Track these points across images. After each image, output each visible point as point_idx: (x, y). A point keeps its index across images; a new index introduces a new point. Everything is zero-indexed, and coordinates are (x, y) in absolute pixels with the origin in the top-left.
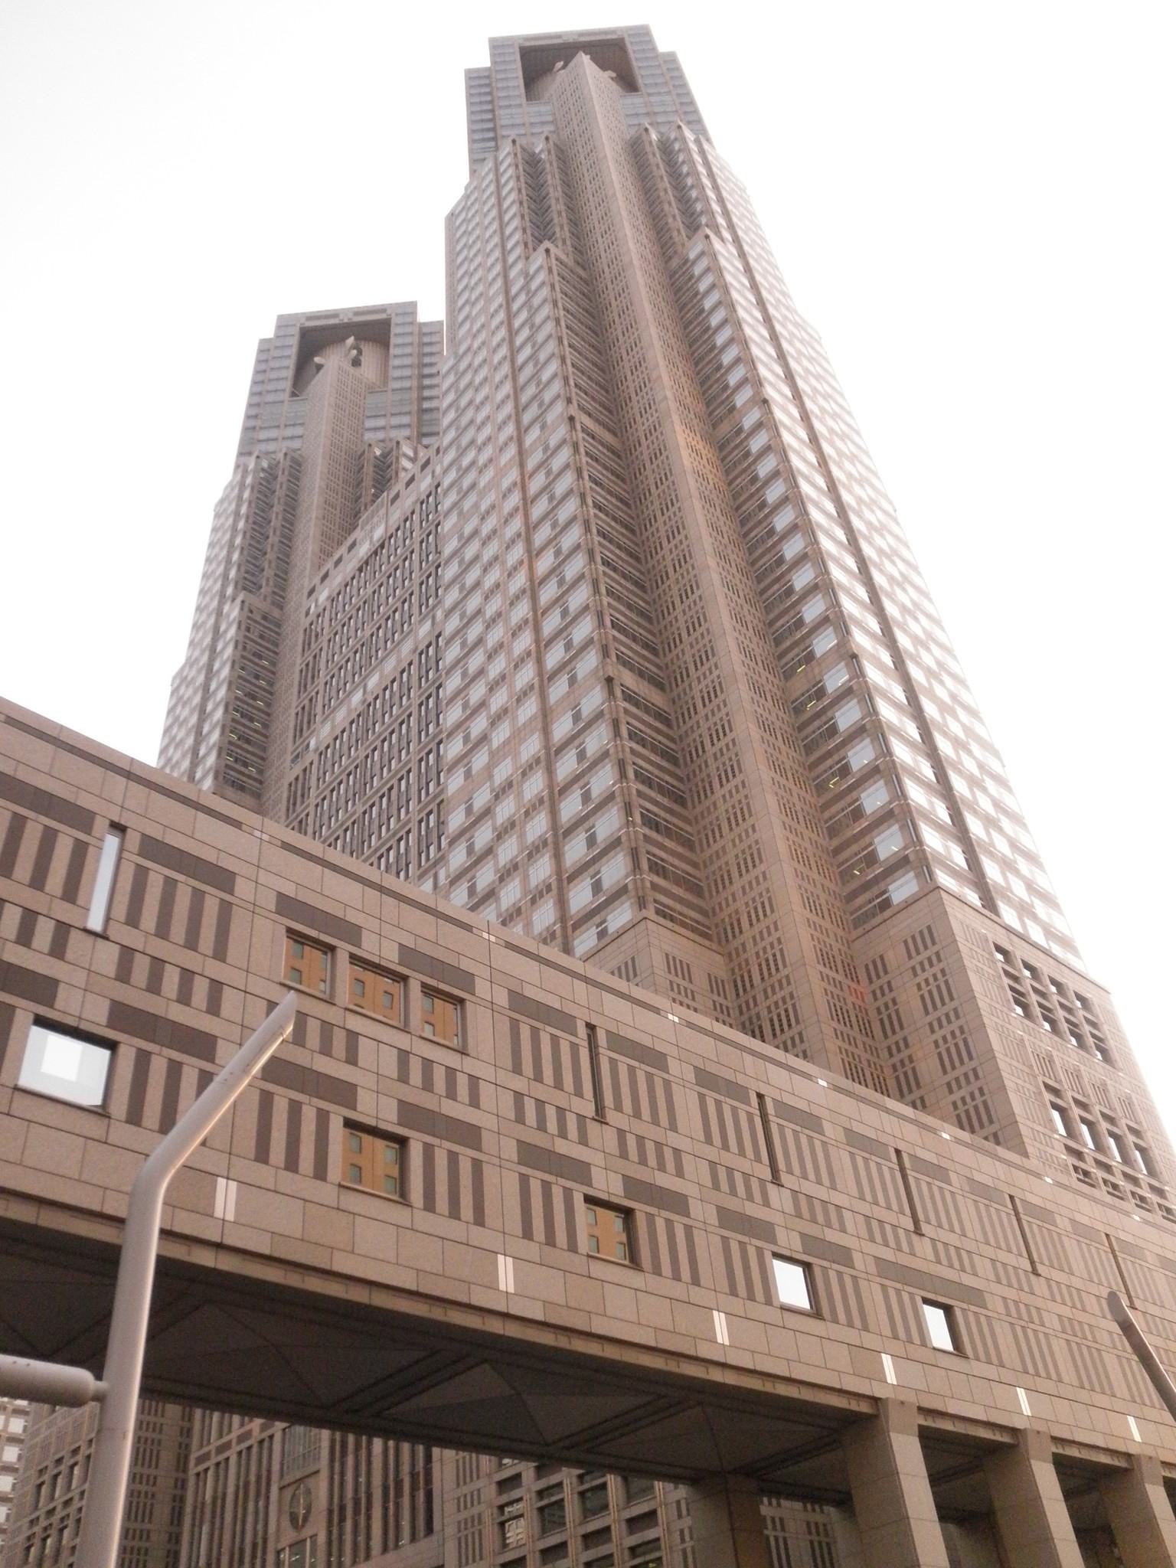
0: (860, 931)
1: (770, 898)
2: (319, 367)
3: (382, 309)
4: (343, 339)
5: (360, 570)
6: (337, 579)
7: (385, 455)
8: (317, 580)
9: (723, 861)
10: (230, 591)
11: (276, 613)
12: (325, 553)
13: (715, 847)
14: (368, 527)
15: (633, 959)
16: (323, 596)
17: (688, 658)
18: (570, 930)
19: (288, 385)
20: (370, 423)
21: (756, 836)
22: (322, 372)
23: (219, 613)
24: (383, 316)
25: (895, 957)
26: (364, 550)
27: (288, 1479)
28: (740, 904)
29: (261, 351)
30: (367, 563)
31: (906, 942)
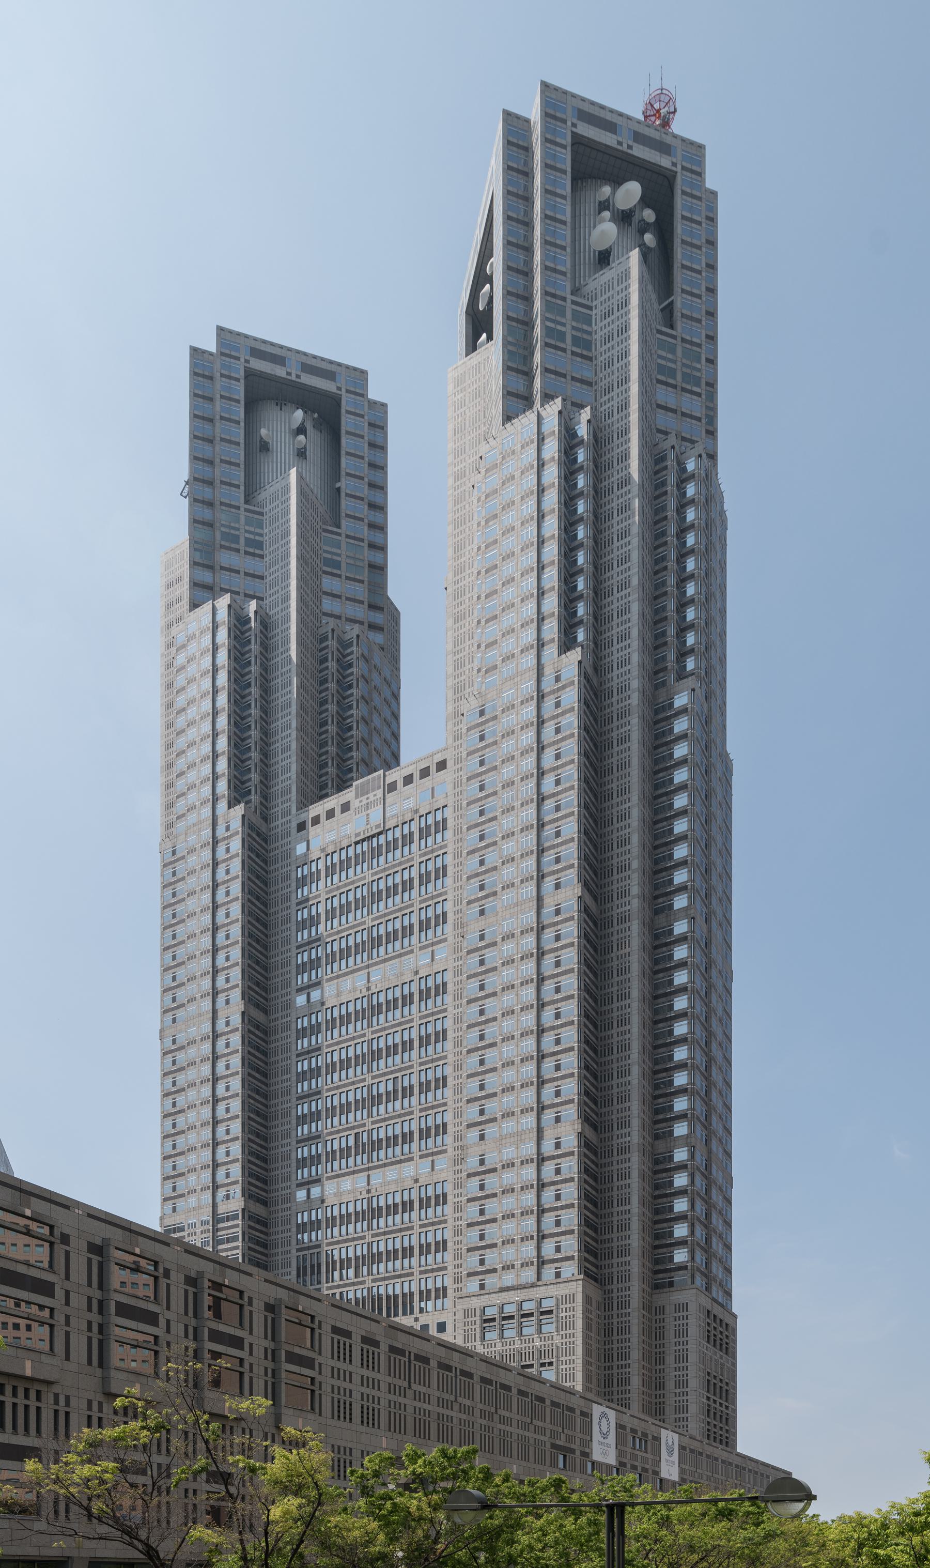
10: (222, 786)
13: (608, 1236)
30: (363, 840)
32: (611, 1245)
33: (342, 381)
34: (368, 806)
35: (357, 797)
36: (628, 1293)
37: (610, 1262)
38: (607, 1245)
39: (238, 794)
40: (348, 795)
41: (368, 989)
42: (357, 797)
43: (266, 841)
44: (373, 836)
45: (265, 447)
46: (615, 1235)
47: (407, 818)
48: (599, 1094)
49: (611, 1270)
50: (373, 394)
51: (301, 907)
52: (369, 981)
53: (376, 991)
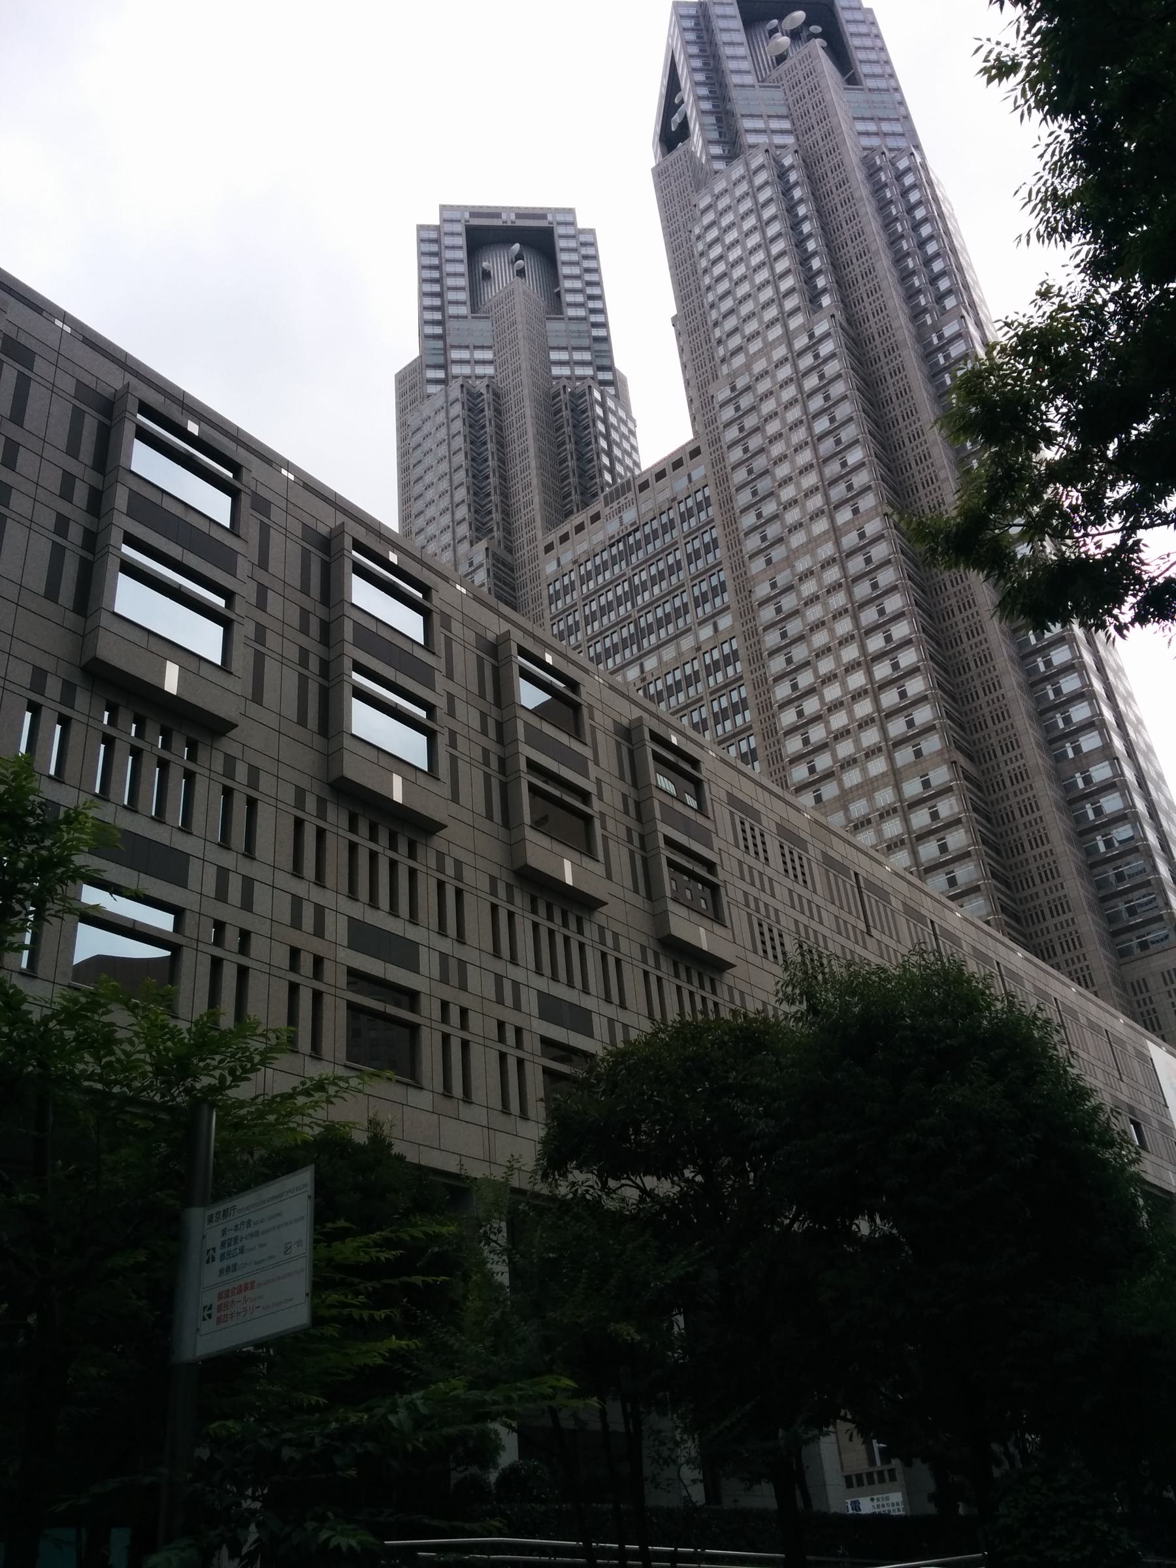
0: (1126, 959)
8: (554, 537)
9: (1037, 903)
10: (463, 530)
11: (508, 558)
13: (1028, 892)
14: (615, 505)
17: (994, 741)
20: (555, 356)
21: (1066, 891)
25: (1154, 983)
29: (421, 241)
30: (619, 541)
31: (1163, 974)
32: (1037, 903)
33: (550, 218)
34: (620, 510)
35: (606, 505)
36: (1083, 964)
37: (1043, 925)
38: (1031, 904)
39: (480, 529)
40: (597, 506)
41: (643, 680)
42: (606, 505)
43: (512, 570)
45: (487, 275)
46: (1039, 888)
47: (664, 508)
48: (965, 719)
50: (581, 225)
51: (555, 620)
52: (642, 671)
53: (653, 679)
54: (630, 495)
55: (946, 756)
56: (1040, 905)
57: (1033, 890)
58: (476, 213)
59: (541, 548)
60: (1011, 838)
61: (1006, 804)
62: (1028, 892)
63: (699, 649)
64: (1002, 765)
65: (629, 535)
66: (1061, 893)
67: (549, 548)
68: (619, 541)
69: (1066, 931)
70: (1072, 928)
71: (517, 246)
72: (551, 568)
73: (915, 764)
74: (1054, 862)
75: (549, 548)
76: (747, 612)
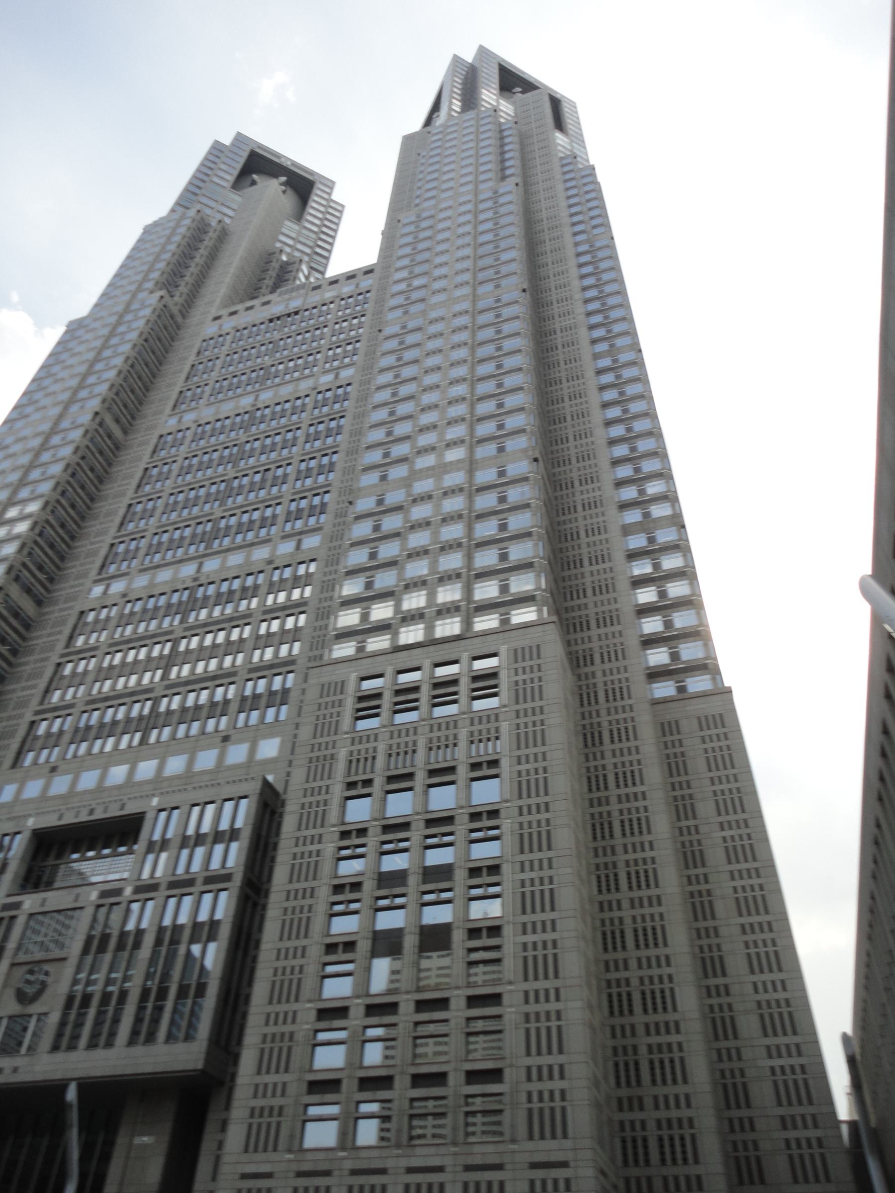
1: (623, 650)
2: (254, 183)
3: (312, 173)
4: (276, 176)
5: (271, 321)
6: (244, 319)
7: (287, 264)
8: (224, 312)
9: (584, 612)
10: (149, 285)
11: (179, 319)
12: (230, 300)
13: (577, 602)
14: (286, 297)
15: (538, 646)
16: (228, 324)
18: (472, 611)
19: (231, 179)
21: (618, 606)
22: (254, 187)
23: (134, 295)
24: (311, 178)
26: (277, 309)
27: (22, 957)
28: (595, 645)
30: (278, 318)
31: (699, 718)
32: (584, 612)
34: (289, 299)
37: (585, 634)
38: (576, 614)
44: (289, 315)
49: (587, 646)
54: (302, 291)
55: (530, 453)
56: (587, 616)
57: (583, 601)
58: (261, 147)
59: (211, 317)
60: (571, 553)
61: (573, 525)
62: (577, 602)
63: (315, 389)
64: (577, 494)
65: (289, 315)
66: (613, 607)
67: (217, 318)
68: (278, 318)
69: (611, 641)
70: (617, 640)
71: (283, 179)
72: (211, 329)
73: (496, 457)
74: (612, 578)
75: (217, 318)
76: (368, 368)
